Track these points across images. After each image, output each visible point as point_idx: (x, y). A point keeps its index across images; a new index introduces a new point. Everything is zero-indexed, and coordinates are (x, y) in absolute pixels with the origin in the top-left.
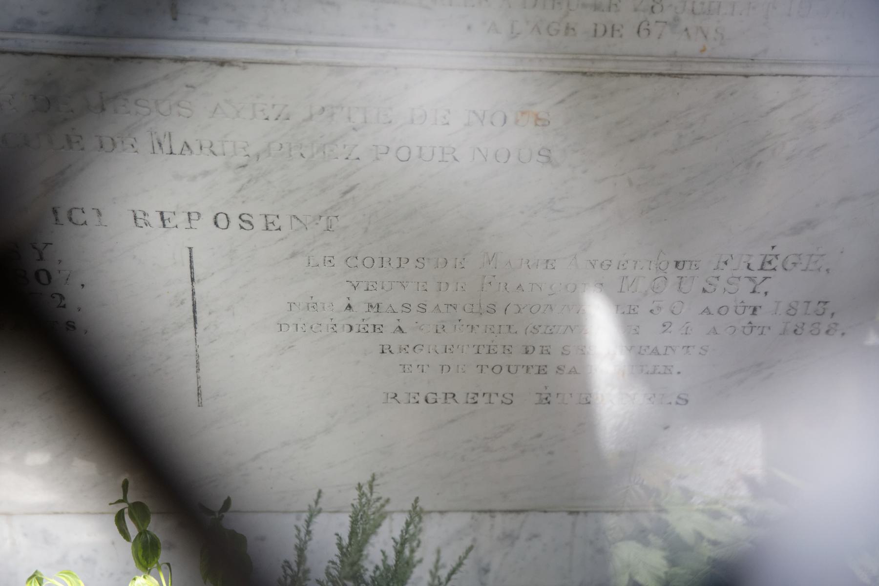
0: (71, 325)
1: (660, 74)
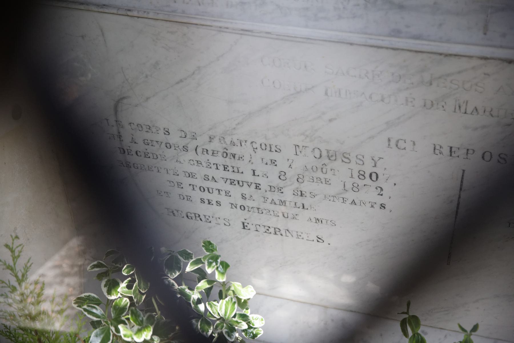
0: (79, 228)
1: (113, 14)
